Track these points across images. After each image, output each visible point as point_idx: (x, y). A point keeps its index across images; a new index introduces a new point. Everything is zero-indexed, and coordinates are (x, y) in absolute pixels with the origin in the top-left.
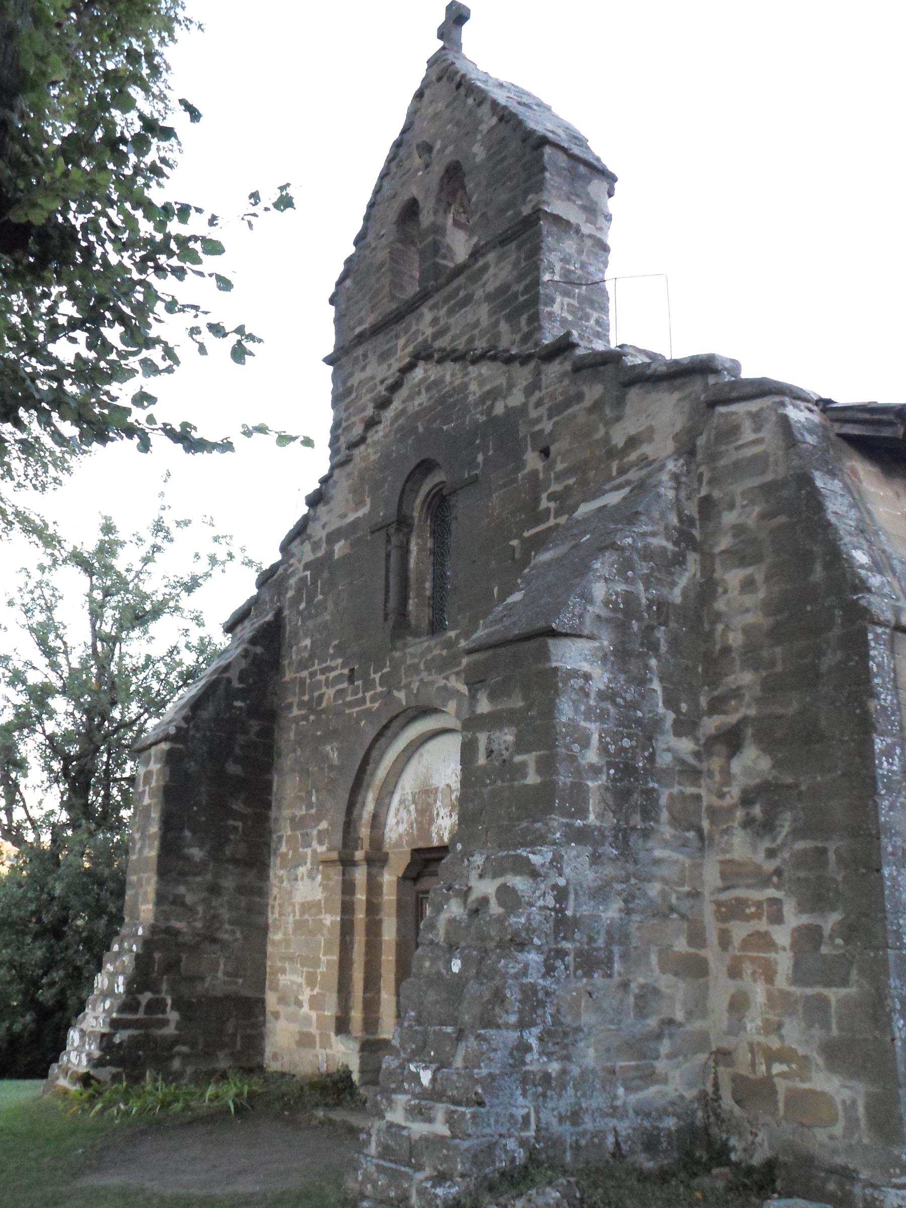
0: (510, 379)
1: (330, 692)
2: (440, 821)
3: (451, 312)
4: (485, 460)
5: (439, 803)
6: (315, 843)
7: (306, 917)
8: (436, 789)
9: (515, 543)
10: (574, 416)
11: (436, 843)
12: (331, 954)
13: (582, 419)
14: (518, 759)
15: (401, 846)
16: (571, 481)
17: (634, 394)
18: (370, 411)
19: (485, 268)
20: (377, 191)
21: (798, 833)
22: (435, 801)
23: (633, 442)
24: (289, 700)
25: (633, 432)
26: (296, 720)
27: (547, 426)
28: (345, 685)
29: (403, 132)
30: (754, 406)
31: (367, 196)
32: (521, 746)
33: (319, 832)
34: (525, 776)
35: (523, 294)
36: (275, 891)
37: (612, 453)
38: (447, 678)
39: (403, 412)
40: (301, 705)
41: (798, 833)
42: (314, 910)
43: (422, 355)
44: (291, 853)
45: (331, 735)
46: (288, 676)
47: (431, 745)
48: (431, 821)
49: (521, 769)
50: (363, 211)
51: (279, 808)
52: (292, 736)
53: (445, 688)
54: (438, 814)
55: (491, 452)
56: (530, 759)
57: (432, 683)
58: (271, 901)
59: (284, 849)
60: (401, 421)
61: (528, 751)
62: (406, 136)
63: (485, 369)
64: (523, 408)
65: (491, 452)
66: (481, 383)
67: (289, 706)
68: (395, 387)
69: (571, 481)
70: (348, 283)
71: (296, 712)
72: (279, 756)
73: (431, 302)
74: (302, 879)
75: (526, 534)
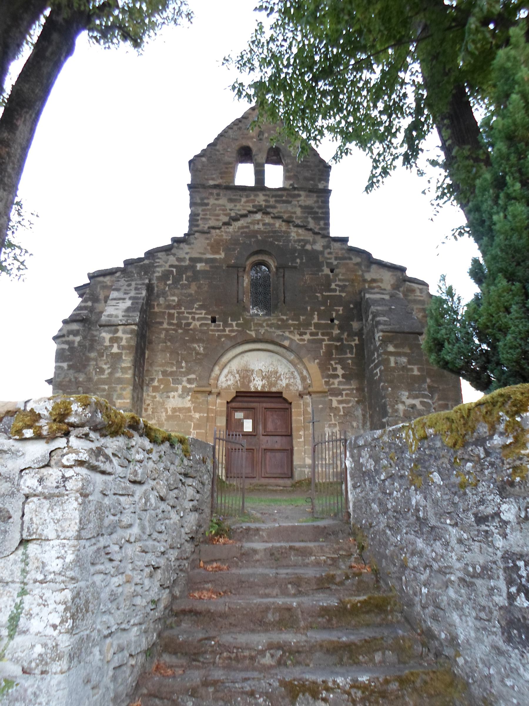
0: (314, 239)
1: (198, 323)
2: (255, 382)
3: (276, 201)
4: (301, 263)
5: (254, 375)
6: (185, 383)
7: (178, 414)
8: (253, 371)
9: (319, 295)
10: (348, 264)
11: (253, 389)
12: (200, 429)
13: (351, 266)
14: (409, 367)
15: (230, 389)
16: (347, 284)
17: (374, 267)
18: (226, 219)
19: (299, 196)
20: (225, 131)
21: (439, 399)
22: (252, 374)
23: (374, 281)
24: (158, 320)
25: (374, 277)
26: (167, 330)
27: (335, 263)
28: (210, 322)
29: (243, 117)
30: (420, 287)
31: (220, 132)
32: (409, 362)
33: (188, 379)
34: (413, 372)
35: (321, 213)
36: (148, 402)
37: (365, 281)
38: (284, 332)
39: (248, 227)
40: (170, 324)
41: (439, 399)
42: (184, 411)
43: (259, 209)
44: (162, 386)
45: (193, 340)
46: (156, 309)
47: (249, 354)
48: (250, 381)
49: (412, 370)
50: (216, 136)
51: (151, 365)
52: (163, 336)
53: (283, 335)
54: (254, 379)
55: (304, 261)
56: (415, 368)
57: (274, 332)
58: (144, 406)
59: (156, 383)
60: (245, 230)
61: (414, 364)
62: (244, 120)
63: (300, 231)
64: (322, 253)
65: (304, 261)
66: (298, 234)
67: (161, 323)
68: (245, 216)
69: (347, 284)
70: (204, 159)
71: (165, 326)
72: (150, 342)
73: (264, 193)
74: (174, 397)
75: (324, 293)
